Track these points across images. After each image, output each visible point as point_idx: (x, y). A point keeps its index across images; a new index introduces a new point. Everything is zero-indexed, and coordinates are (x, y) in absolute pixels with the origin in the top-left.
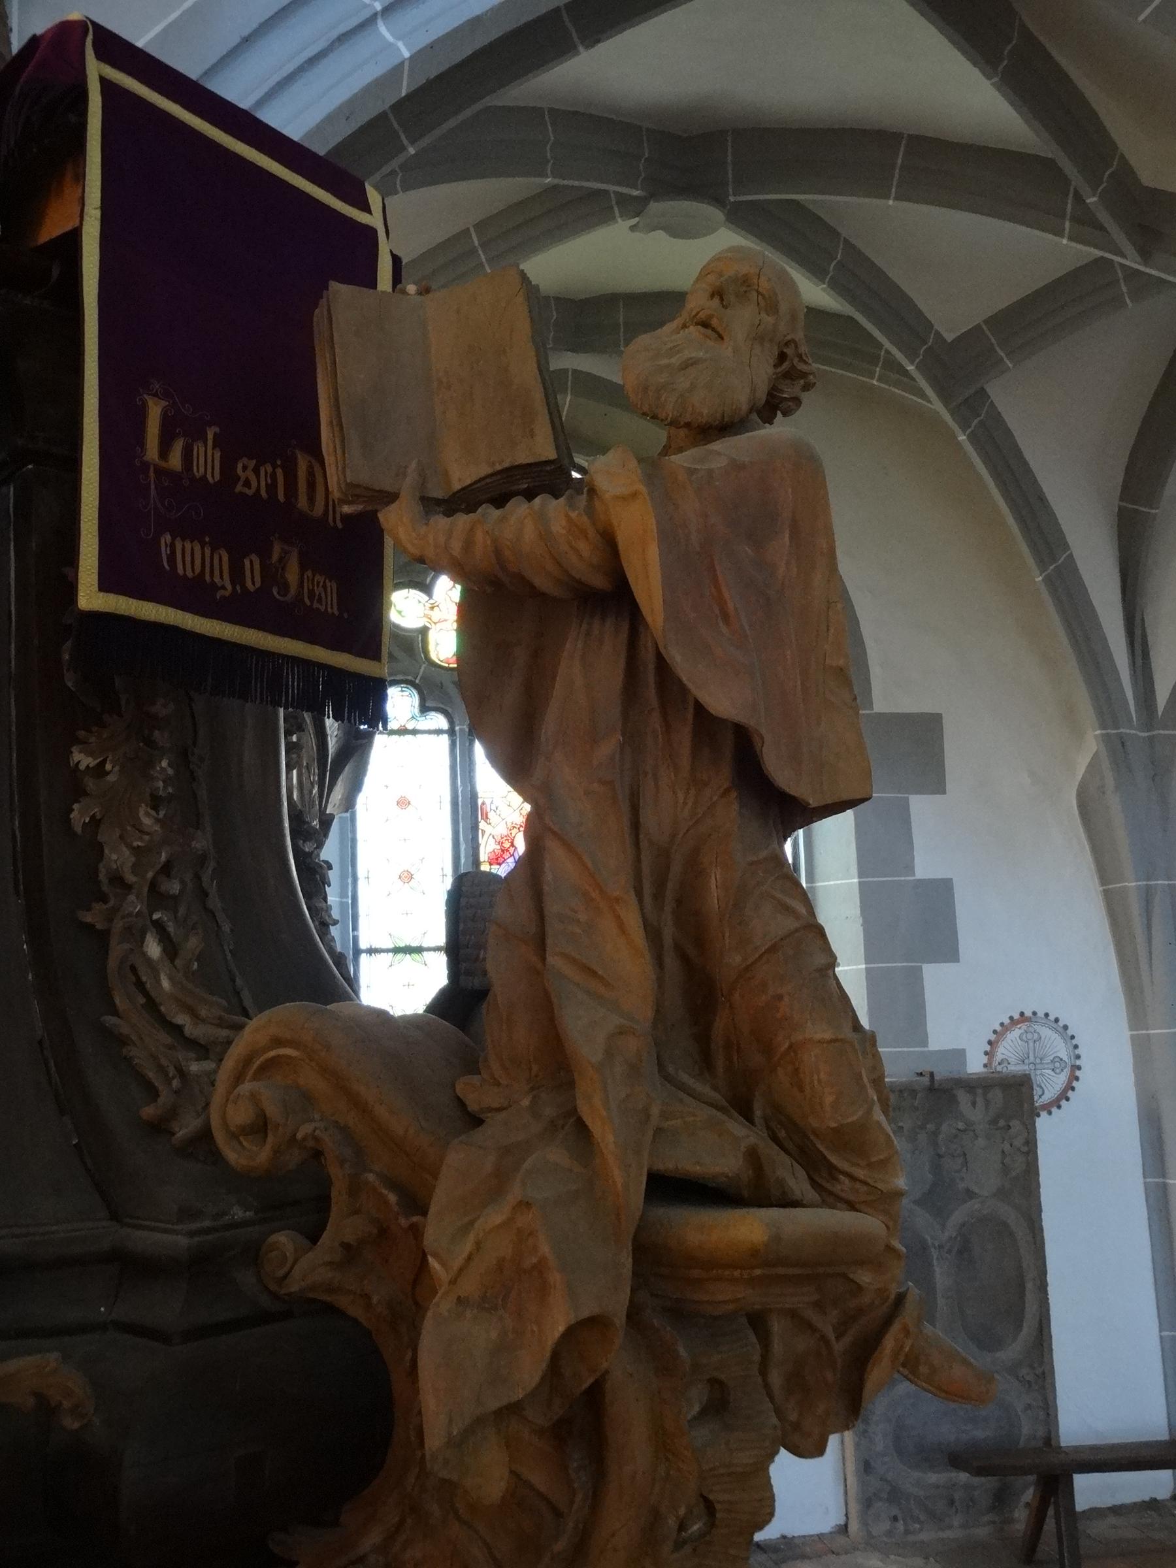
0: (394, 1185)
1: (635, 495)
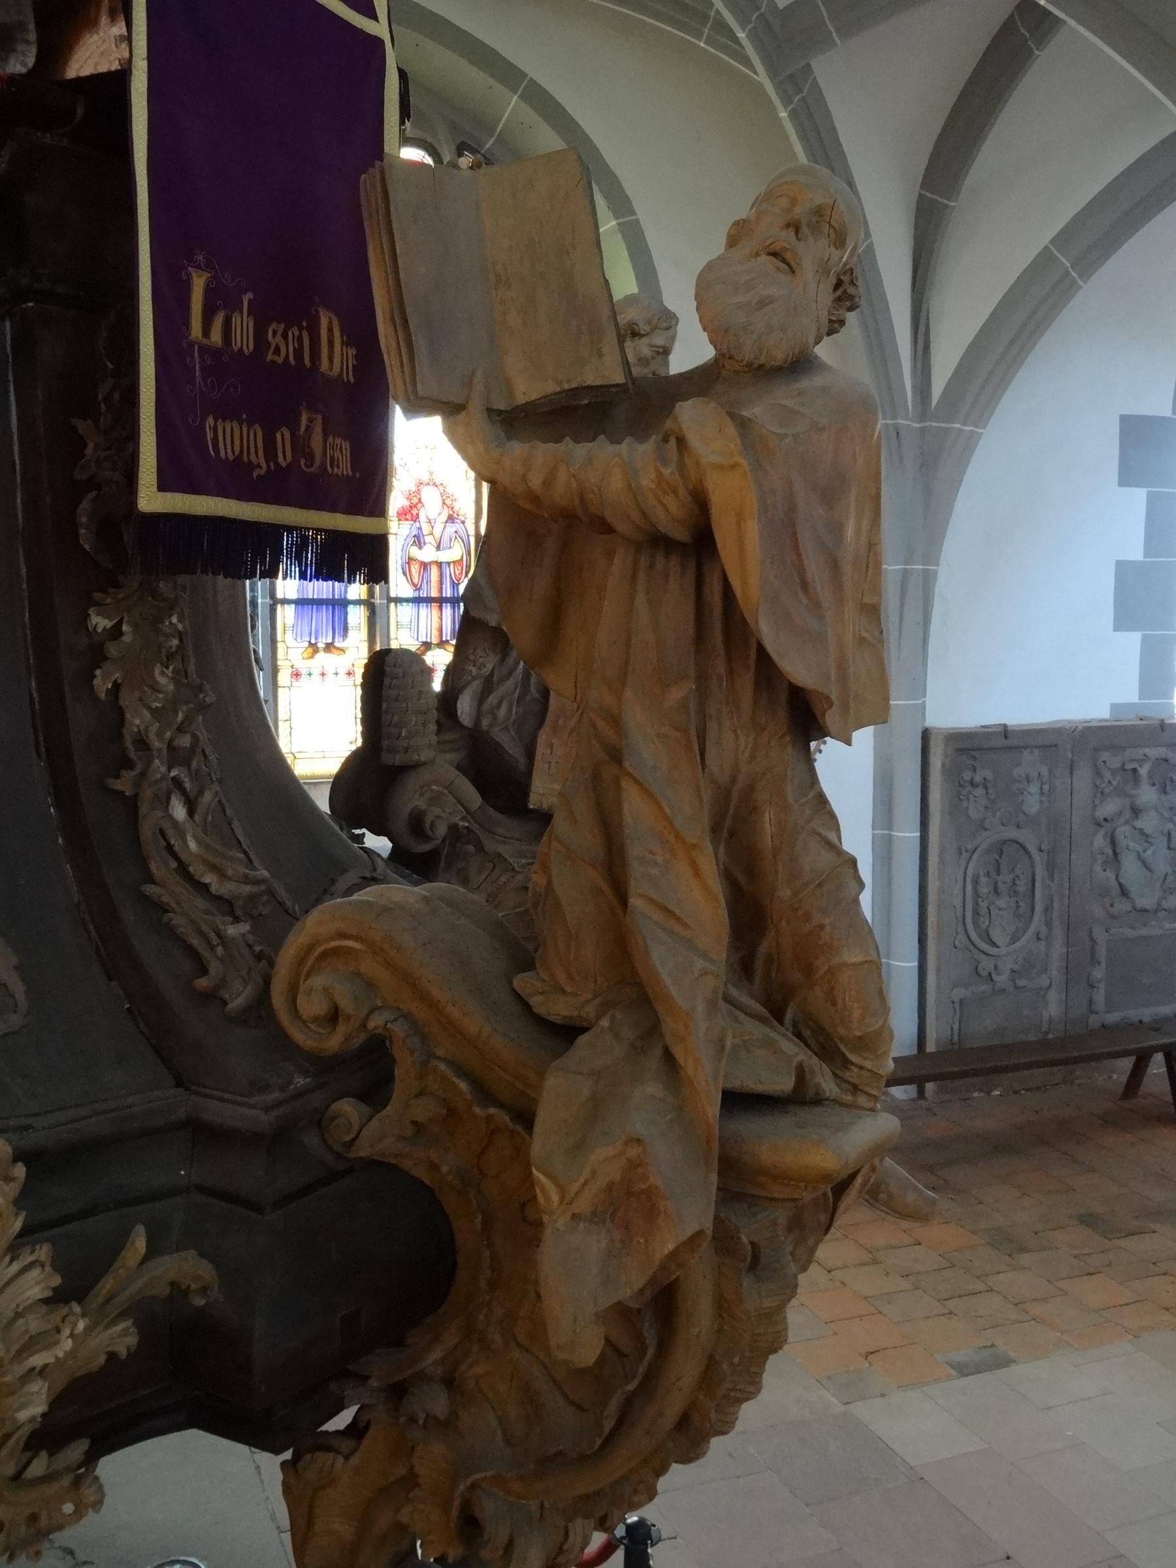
0: (462, 1071)
1: (734, 467)
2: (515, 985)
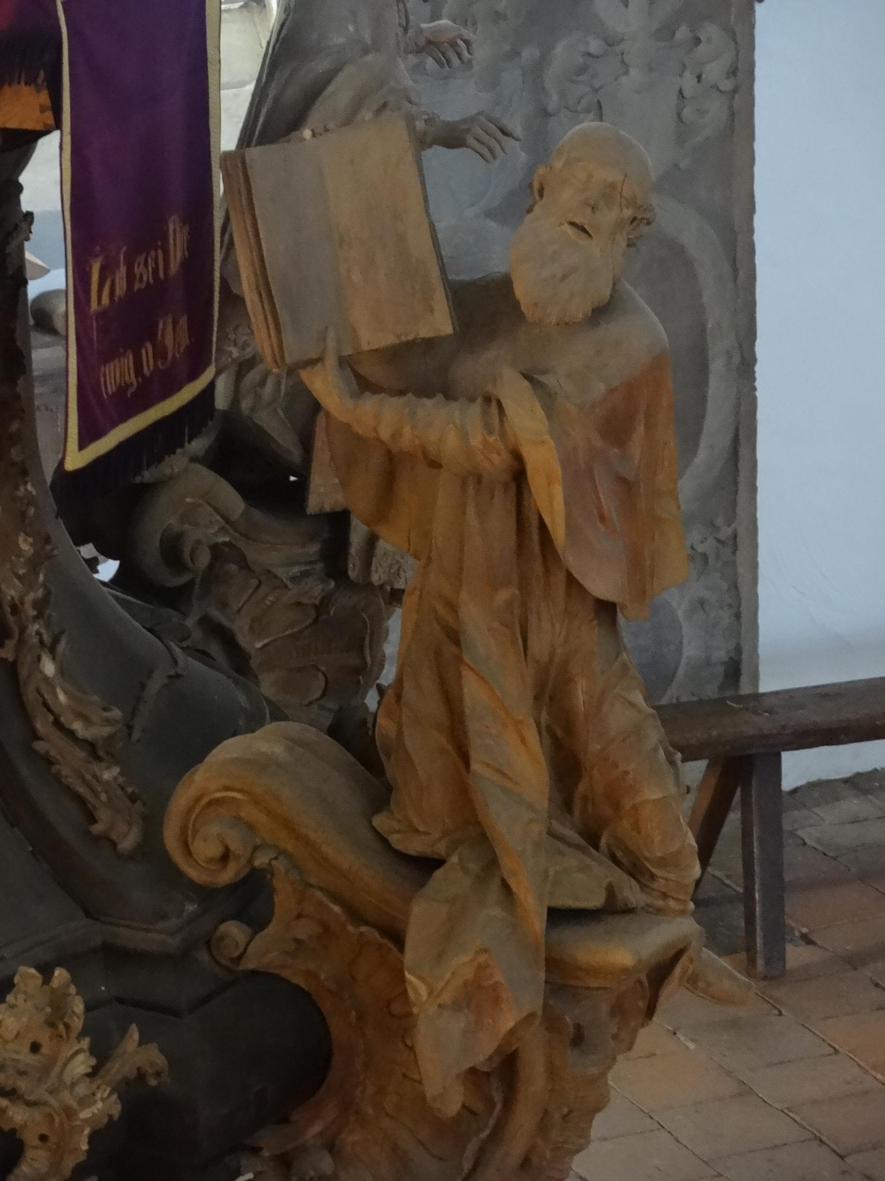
0: (336, 898)
2: (374, 824)
